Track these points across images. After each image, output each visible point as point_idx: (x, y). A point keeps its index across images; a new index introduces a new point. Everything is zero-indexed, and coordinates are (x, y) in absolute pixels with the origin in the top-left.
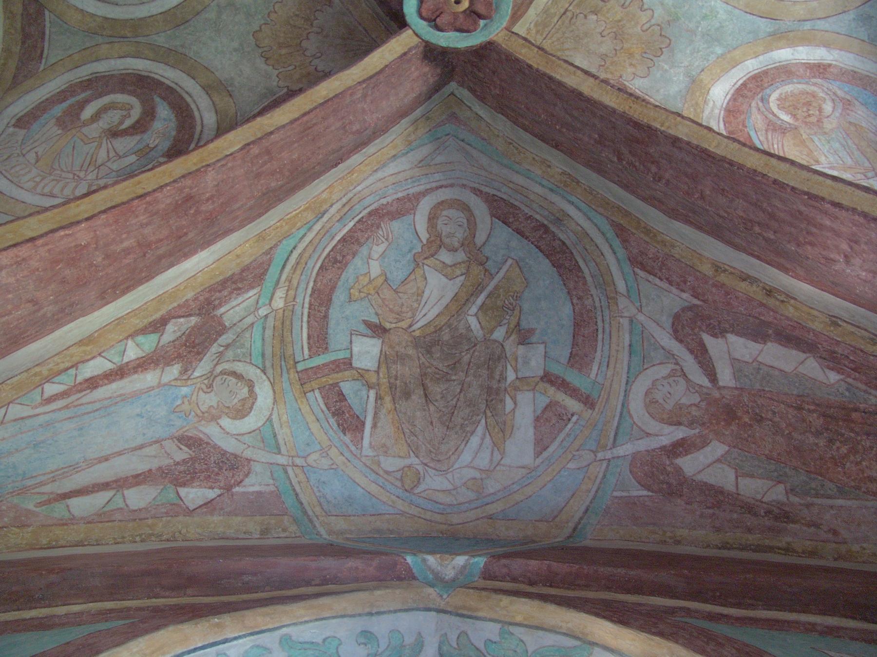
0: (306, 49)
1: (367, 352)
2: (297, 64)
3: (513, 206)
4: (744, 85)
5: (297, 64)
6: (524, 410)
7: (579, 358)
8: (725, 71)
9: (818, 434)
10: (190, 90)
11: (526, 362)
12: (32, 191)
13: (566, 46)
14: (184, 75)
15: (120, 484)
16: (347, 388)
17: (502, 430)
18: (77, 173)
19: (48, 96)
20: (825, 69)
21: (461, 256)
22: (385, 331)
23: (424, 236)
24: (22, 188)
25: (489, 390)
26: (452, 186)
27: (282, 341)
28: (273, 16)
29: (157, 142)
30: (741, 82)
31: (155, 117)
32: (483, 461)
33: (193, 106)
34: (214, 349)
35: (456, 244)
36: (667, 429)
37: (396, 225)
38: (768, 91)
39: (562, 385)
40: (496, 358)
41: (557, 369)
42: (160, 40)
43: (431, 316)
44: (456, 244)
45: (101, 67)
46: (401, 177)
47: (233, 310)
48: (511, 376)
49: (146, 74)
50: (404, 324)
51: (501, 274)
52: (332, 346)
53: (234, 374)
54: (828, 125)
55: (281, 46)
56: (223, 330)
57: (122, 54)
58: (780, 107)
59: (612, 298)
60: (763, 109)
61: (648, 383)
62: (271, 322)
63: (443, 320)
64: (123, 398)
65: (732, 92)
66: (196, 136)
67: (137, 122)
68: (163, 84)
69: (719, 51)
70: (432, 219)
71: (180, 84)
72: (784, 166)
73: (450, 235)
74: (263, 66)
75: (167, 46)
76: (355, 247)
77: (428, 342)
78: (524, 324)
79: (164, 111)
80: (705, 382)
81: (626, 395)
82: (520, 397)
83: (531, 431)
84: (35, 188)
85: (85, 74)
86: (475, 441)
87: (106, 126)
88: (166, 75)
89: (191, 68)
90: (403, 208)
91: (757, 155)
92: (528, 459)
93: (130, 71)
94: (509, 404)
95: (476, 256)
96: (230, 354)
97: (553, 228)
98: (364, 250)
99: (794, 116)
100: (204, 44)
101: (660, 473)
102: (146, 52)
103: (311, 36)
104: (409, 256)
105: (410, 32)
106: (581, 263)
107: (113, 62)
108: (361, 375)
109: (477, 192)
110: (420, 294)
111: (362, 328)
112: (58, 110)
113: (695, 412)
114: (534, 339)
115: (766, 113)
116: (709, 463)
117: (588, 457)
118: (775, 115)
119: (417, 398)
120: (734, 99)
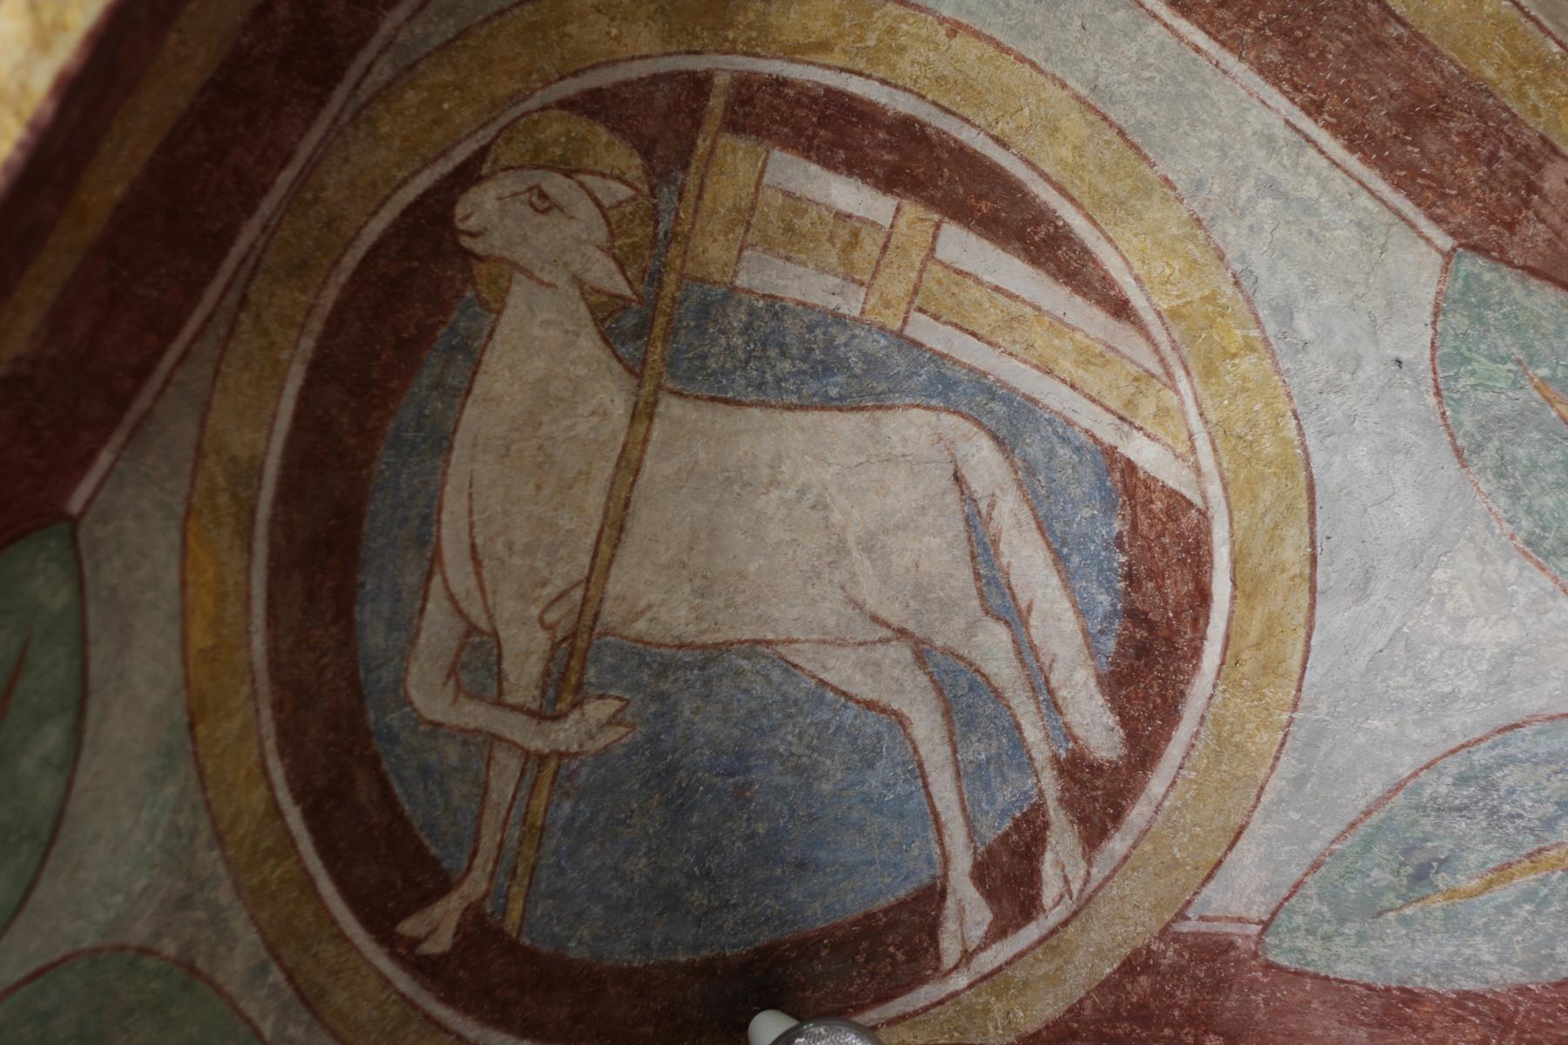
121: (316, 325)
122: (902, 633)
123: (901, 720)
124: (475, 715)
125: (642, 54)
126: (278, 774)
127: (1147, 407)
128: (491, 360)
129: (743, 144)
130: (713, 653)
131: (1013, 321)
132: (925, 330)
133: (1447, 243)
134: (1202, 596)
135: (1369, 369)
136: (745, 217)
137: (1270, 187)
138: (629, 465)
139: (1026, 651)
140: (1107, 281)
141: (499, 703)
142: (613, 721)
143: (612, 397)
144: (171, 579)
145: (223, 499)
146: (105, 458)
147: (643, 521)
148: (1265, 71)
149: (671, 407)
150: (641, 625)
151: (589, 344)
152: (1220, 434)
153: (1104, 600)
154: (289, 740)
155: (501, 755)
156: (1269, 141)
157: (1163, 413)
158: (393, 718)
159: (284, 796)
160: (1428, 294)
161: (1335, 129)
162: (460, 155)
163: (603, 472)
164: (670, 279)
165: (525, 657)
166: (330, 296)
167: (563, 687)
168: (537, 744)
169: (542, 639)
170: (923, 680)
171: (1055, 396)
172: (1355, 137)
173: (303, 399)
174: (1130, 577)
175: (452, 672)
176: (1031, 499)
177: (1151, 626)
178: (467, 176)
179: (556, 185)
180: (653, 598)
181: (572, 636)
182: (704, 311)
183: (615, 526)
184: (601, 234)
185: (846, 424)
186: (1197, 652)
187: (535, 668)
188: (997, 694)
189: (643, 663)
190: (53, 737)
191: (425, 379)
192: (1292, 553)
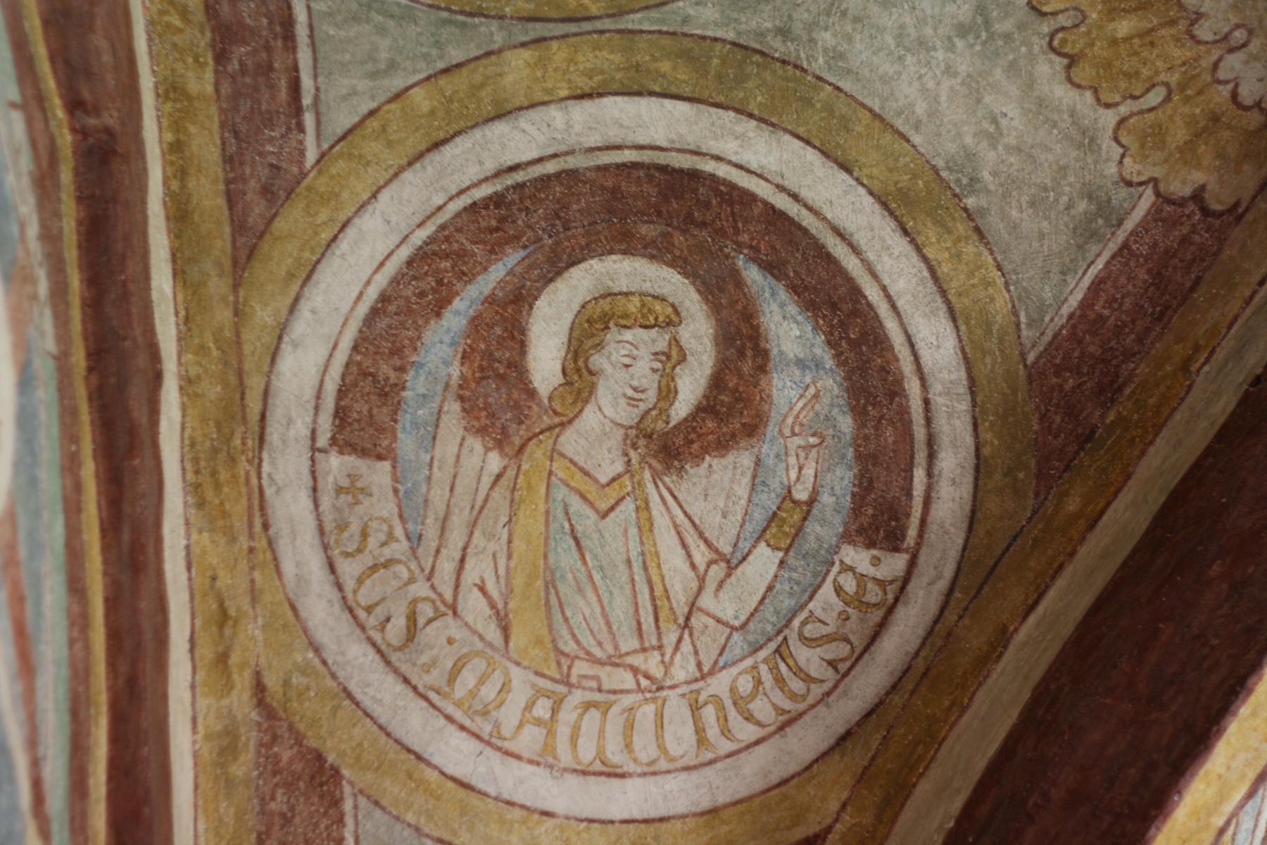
0: (1199, 16)
2: (1174, 79)
5: (1174, 79)
10: (848, 222)
12: (544, 759)
14: (811, 155)
18: (637, 660)
19: (382, 280)
24: (518, 757)
29: (809, 472)
31: (765, 354)
33: (872, 293)
45: (521, 142)
49: (685, 162)
57: (584, 84)
66: (920, 433)
67: (717, 382)
68: (748, 198)
71: (804, 193)
74: (1062, 93)
75: (731, 36)
79: (788, 330)
84: (549, 747)
85: (473, 172)
87: (627, 415)
88: (751, 158)
93: (629, 156)
100: (857, 20)
102: (665, 66)
107: (555, 114)
112: (441, 347)
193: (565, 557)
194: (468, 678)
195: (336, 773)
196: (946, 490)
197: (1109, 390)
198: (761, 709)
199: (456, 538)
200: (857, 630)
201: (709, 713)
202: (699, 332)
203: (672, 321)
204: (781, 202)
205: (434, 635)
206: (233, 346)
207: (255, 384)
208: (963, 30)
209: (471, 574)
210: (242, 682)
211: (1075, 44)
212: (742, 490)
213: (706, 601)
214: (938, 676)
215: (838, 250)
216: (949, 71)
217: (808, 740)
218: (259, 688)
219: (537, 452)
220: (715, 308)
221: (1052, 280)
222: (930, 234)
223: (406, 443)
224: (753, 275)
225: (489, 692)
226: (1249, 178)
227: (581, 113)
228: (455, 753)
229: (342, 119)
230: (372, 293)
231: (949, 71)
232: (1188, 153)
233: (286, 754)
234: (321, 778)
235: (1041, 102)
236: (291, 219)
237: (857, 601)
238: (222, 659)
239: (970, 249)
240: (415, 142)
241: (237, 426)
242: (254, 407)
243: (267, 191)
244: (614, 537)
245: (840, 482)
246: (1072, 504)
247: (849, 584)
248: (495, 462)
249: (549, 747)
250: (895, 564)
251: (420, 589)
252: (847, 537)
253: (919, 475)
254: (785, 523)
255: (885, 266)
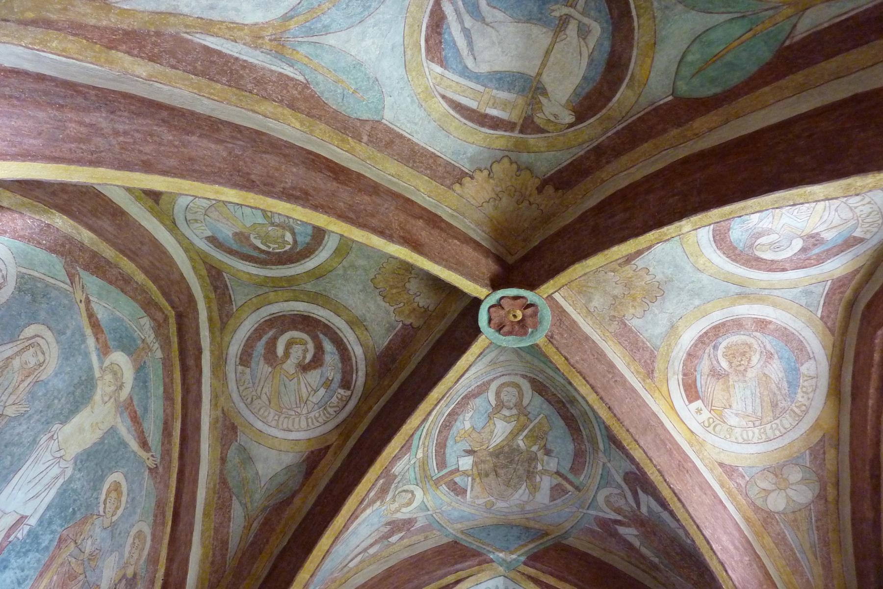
1: (466, 463)
3: (545, 386)
4: (706, 333)
6: (546, 483)
7: (576, 468)
8: (697, 319)
9: (677, 554)
10: (340, 327)
11: (548, 463)
13: (590, 284)
15: (365, 550)
16: (457, 480)
17: (534, 489)
19: (249, 334)
20: (766, 326)
21: (514, 411)
22: (475, 452)
23: (493, 403)
25: (529, 471)
26: (509, 374)
27: (424, 470)
28: (383, 270)
30: (705, 330)
32: (525, 498)
33: (345, 340)
34: (393, 486)
35: (512, 406)
36: (613, 513)
37: (477, 400)
38: (720, 340)
39: (566, 479)
40: (532, 459)
41: (563, 471)
42: (309, 287)
43: (498, 442)
44: (512, 406)
46: (479, 374)
47: (397, 469)
48: (540, 467)
50: (484, 447)
51: (536, 421)
52: (448, 465)
53: (404, 491)
54: (750, 374)
55: (392, 287)
56: (396, 477)
58: (725, 355)
59: (596, 449)
60: (712, 356)
61: (608, 494)
62: (417, 464)
63: (505, 443)
64: (359, 524)
65: (696, 338)
66: (355, 368)
67: (314, 356)
68: (320, 321)
69: (697, 302)
70: (498, 394)
72: (679, 505)
73: (509, 401)
74: (383, 304)
76: (456, 417)
77: (497, 453)
78: (548, 446)
79: (328, 346)
80: (634, 506)
81: (596, 493)
82: (543, 477)
83: (548, 492)
85: (265, 314)
86: (521, 491)
87: (296, 361)
89: (337, 308)
90: (482, 389)
91: (669, 491)
92: (546, 501)
94: (538, 479)
95: (522, 411)
96: (401, 484)
97: (568, 406)
98: (461, 417)
99: (731, 363)
101: (607, 527)
103: (411, 280)
104: (486, 415)
105: (483, 337)
106: (582, 428)
107: (281, 304)
108: (465, 473)
109: (524, 376)
110: (492, 432)
111: (463, 454)
112: (260, 347)
113: (627, 513)
114: (553, 455)
115: (713, 359)
116: (629, 533)
117: (574, 509)
118: (718, 362)
119: (492, 476)
120: (695, 345)
121: (608, 107)
122: (487, 25)
123: (488, 4)
124: (586, 20)
125: (532, 139)
126: (636, 24)
127: (439, 79)
128: (571, 91)
129: (513, 120)
130: (528, 21)
131: (464, 91)
132: (480, 88)
133: (384, 121)
134: (427, 41)
135: (396, 94)
136: (514, 107)
137: (416, 124)
138: (543, 65)
139: (461, 22)
140: (446, 102)
141: (580, 22)
142: (553, 11)
143: (546, 78)
144: (652, 74)
145: (636, 84)
146: (661, 102)
147: (542, 53)
148: (418, 145)
149: (533, 74)
150: (544, 30)
151: (549, 89)
152: (424, 75)
153: (446, 37)
154: (632, 30)
155: (581, 10)
156: (417, 132)
157: (435, 78)
158: (605, 25)
159: (635, 19)
160: (386, 110)
161: (405, 137)
162: (572, 129)
163: (549, 64)
164: (530, 96)
165: (572, 30)
166: (604, 111)
167: (564, 21)
168: (572, 10)
169: (568, 32)
170: (483, 14)
171: (456, 78)
172: (401, 137)
173: (614, 96)
174: (441, 42)
175: (590, 31)
176: (460, 56)
177: (437, 33)
178: (571, 125)
179: (552, 119)
180: (542, 36)
181: (560, 31)
182: (523, 90)
183: (548, 53)
184: (544, 108)
185: (497, 68)
186: (427, 27)
187: (570, 27)
188: (468, 12)
189: (545, 22)
190: (690, 58)
191: (587, 90)
192: (409, 52)
193: (282, 389)
194: (262, 411)
195: (236, 427)
196: (360, 379)
197: (394, 360)
198: (320, 420)
199: (262, 383)
200: (341, 405)
201: (310, 420)
202: (311, 346)
203: (306, 343)
204: (327, 322)
205: (256, 402)
206: (220, 345)
207: (225, 352)
208: (361, 291)
209: (264, 391)
210: (220, 409)
211: (384, 294)
212: (319, 377)
213: (310, 398)
214: (357, 414)
215: (338, 332)
216: (359, 298)
217: (330, 426)
218: (223, 410)
219: (278, 368)
220: (314, 342)
221: (381, 339)
222: (356, 329)
223: (253, 365)
224: (321, 336)
225: (266, 414)
226: (422, 321)
227: (286, 304)
228: (259, 425)
229: (240, 304)
230: (247, 336)
231: (359, 298)
232: (409, 316)
233: (227, 423)
234: (234, 428)
235: (378, 305)
236: (232, 321)
237: (341, 400)
238: (216, 405)
239: (365, 332)
240: (254, 308)
241: (219, 361)
242: (224, 356)
243: (227, 316)
244: (293, 385)
245: (338, 377)
246: (386, 383)
247: (339, 396)
248: (270, 369)
249: (277, 425)
250: (349, 393)
251: (254, 393)
252: (339, 387)
253: (354, 375)
254: (327, 384)
255: (347, 335)
